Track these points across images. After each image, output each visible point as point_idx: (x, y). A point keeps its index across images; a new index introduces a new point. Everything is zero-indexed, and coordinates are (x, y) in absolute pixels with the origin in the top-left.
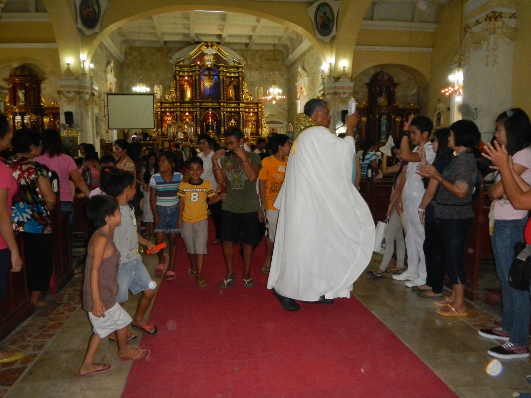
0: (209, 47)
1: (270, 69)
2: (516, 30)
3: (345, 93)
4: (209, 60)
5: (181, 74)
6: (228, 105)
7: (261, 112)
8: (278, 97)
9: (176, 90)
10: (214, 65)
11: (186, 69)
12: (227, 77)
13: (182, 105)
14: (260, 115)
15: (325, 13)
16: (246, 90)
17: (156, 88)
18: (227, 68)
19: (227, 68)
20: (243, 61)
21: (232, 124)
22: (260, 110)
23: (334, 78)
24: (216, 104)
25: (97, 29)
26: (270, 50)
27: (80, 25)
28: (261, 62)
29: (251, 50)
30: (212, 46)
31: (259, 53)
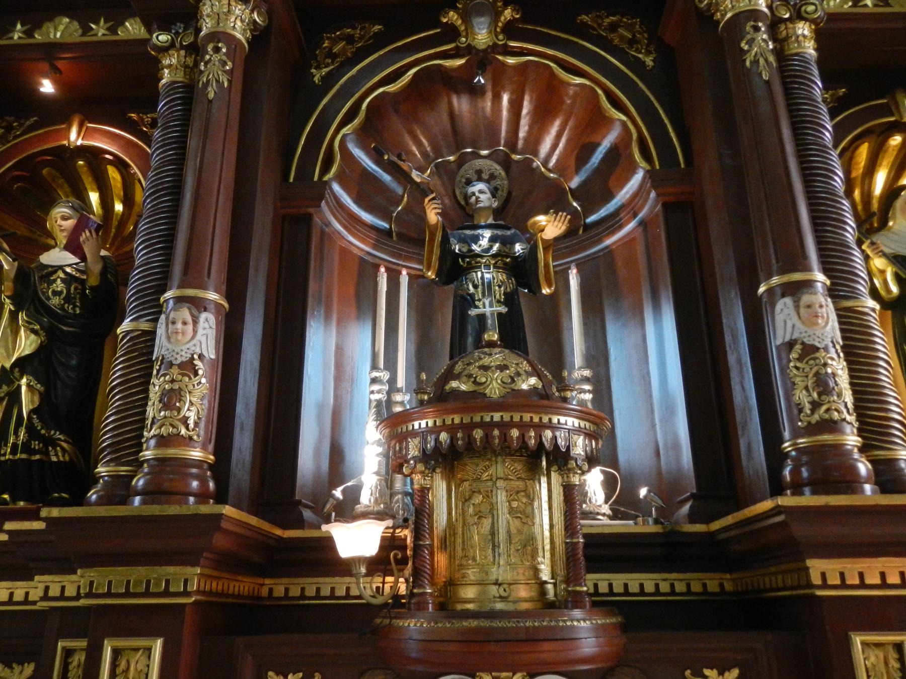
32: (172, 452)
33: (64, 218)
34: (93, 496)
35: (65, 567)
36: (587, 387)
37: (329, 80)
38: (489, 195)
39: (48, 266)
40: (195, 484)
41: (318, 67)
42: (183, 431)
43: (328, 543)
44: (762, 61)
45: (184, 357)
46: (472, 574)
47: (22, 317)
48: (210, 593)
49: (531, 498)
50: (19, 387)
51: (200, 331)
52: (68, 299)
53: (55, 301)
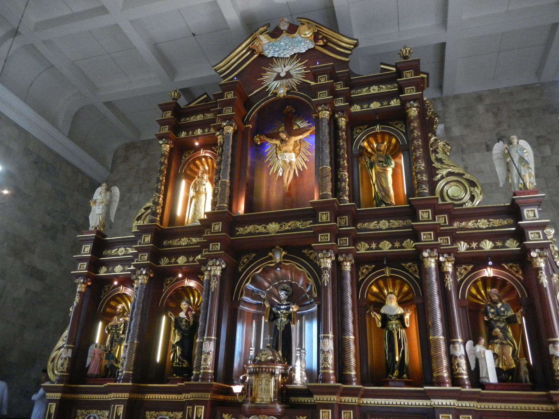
0: (284, 35)
1: (538, 138)
4: (283, 75)
5: (183, 134)
6: (359, 225)
7: (543, 247)
10: (297, 86)
11: (200, 117)
13: (165, 243)
14: (541, 264)
17: (99, 195)
21: (385, 319)
24: (298, 224)
26: (526, 87)
28: (499, 124)
29: (456, 97)
30: (293, 29)
31: (487, 101)
32: (206, 371)
33: (185, 305)
34: (192, 378)
35: (188, 392)
36: (298, 352)
37: (243, 270)
38: (285, 295)
39: (181, 318)
40: (210, 377)
41: (240, 267)
42: (208, 366)
43: (231, 389)
44: (326, 281)
45: (207, 351)
46: (259, 396)
47: (176, 331)
48: (213, 398)
49: (270, 382)
50: (176, 349)
51: (211, 346)
52: (186, 327)
53: (183, 327)
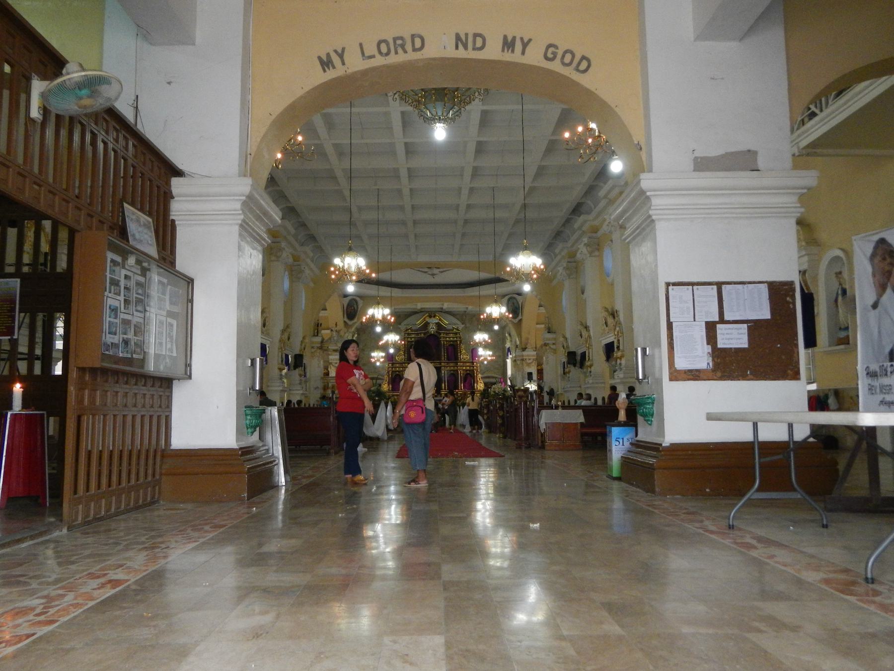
2: (555, 350)
3: (530, 359)
8: (489, 358)
9: (404, 353)
11: (413, 336)
12: (447, 341)
15: (514, 304)
16: (464, 351)
18: (447, 334)
19: (447, 334)
20: (463, 324)
22: (475, 368)
23: (522, 348)
25: (355, 320)
27: (346, 319)
30: (434, 317)
